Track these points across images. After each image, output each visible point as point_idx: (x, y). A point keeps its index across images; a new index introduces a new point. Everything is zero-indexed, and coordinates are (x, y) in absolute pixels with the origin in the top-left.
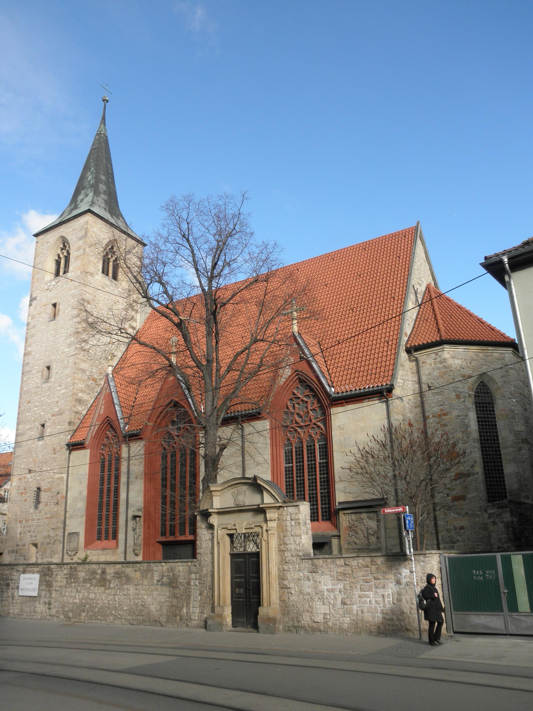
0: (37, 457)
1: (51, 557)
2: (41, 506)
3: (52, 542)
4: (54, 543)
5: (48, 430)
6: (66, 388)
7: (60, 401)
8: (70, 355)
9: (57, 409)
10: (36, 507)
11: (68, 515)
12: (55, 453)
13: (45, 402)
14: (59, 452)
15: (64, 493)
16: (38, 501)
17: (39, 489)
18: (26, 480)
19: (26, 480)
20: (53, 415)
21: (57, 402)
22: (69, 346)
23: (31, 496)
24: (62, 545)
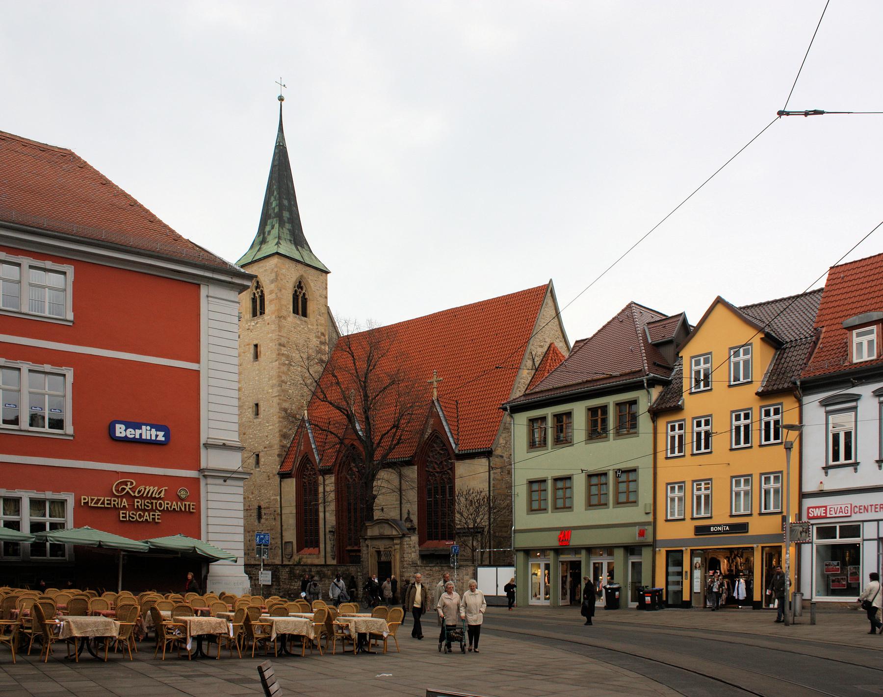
0: (256, 481)
1: (274, 559)
2: (263, 521)
3: (273, 548)
4: (275, 549)
5: (262, 460)
6: (273, 425)
7: (269, 436)
8: (273, 395)
9: (268, 443)
10: (259, 522)
11: (283, 529)
12: (269, 479)
13: (257, 436)
14: (272, 478)
15: (279, 511)
16: (259, 517)
17: (260, 508)
18: (249, 499)
19: (249, 499)
20: (265, 448)
21: (267, 436)
22: (272, 387)
23: (255, 514)
24: (281, 551)
